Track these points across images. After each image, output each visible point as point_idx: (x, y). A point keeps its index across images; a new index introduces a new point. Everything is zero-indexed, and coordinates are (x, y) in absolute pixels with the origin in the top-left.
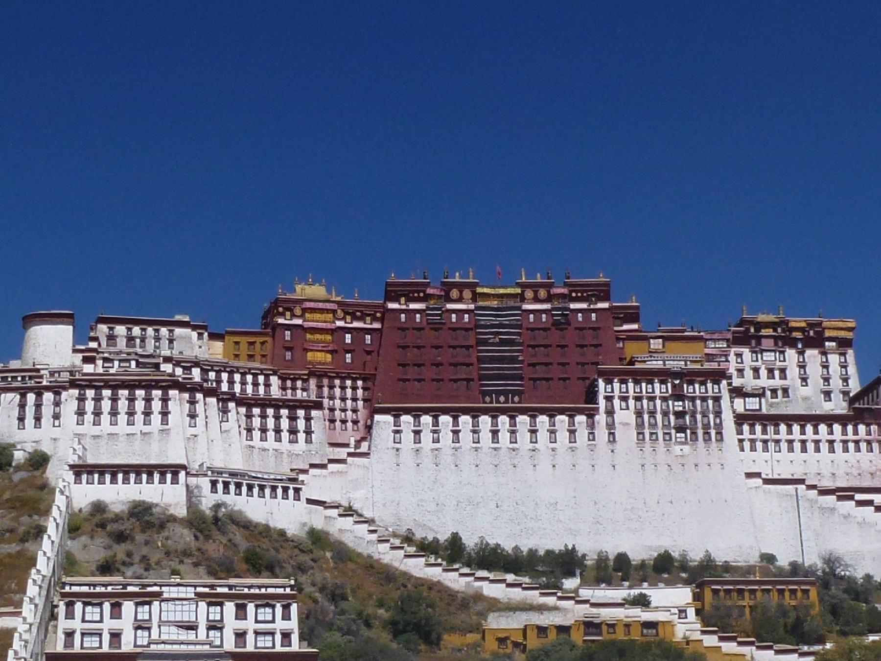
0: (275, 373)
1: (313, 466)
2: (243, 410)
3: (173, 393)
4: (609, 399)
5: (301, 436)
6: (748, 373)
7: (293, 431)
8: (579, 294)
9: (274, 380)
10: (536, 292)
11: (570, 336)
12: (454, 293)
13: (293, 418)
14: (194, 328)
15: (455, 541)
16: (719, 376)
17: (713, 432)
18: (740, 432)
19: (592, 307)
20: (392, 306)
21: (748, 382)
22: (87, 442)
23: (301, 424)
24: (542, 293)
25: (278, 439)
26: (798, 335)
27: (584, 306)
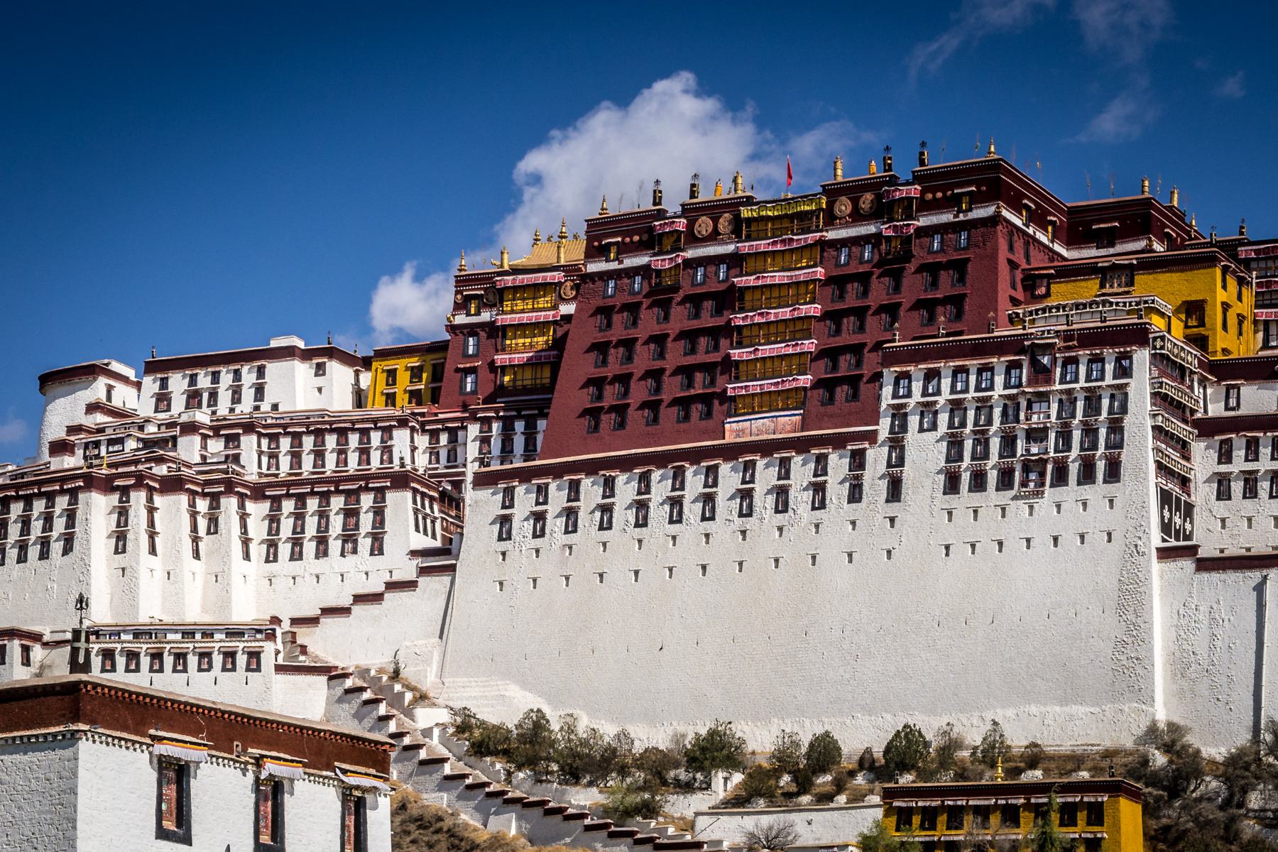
0: (403, 423)
1: (359, 599)
2: (265, 507)
4: (899, 414)
5: (365, 544)
7: (349, 538)
8: (939, 195)
9: (401, 438)
10: (855, 202)
11: (913, 286)
13: (351, 513)
14: (306, 355)
15: (536, 728)
17: (1101, 466)
19: (961, 217)
23: (366, 521)
27: (946, 217)
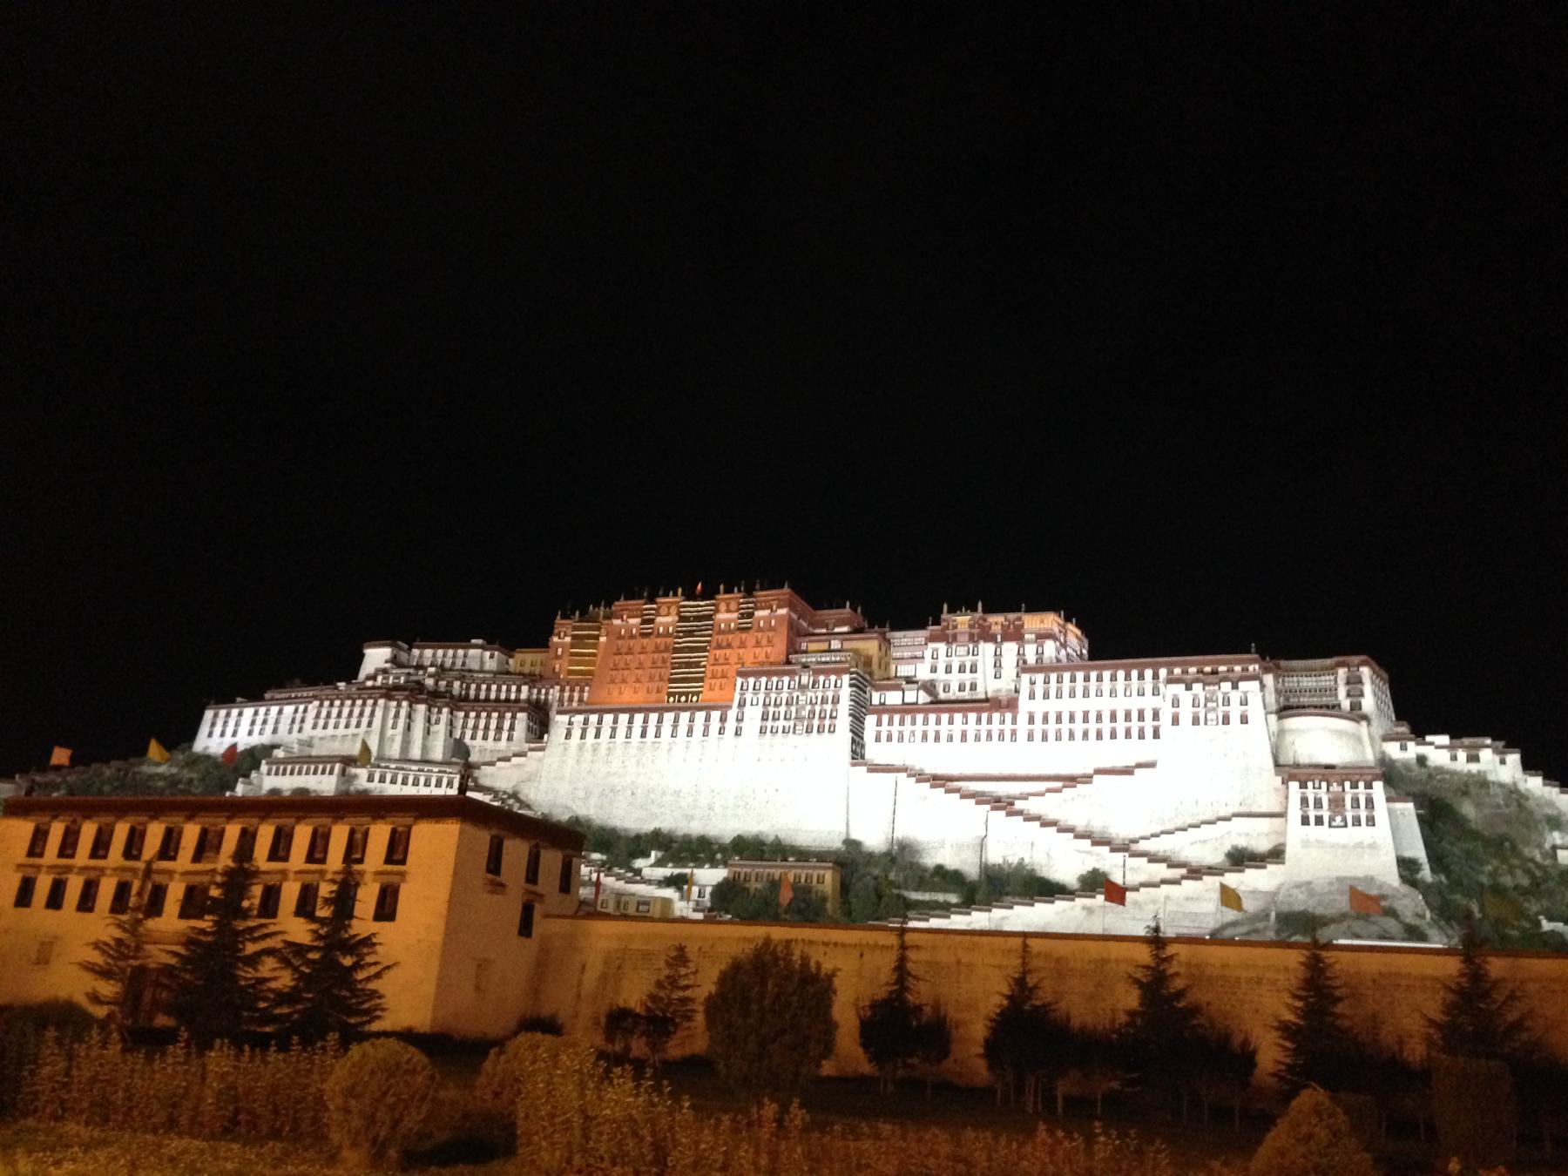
3: (381, 702)
5: (505, 735)
6: (941, 667)
7: (499, 729)
12: (664, 610)
16: (839, 672)
18: (879, 723)
20: (617, 622)
21: (941, 675)
22: (316, 741)
23: (507, 724)
24: (733, 606)
25: (485, 738)
26: (996, 629)
27: (767, 612)
